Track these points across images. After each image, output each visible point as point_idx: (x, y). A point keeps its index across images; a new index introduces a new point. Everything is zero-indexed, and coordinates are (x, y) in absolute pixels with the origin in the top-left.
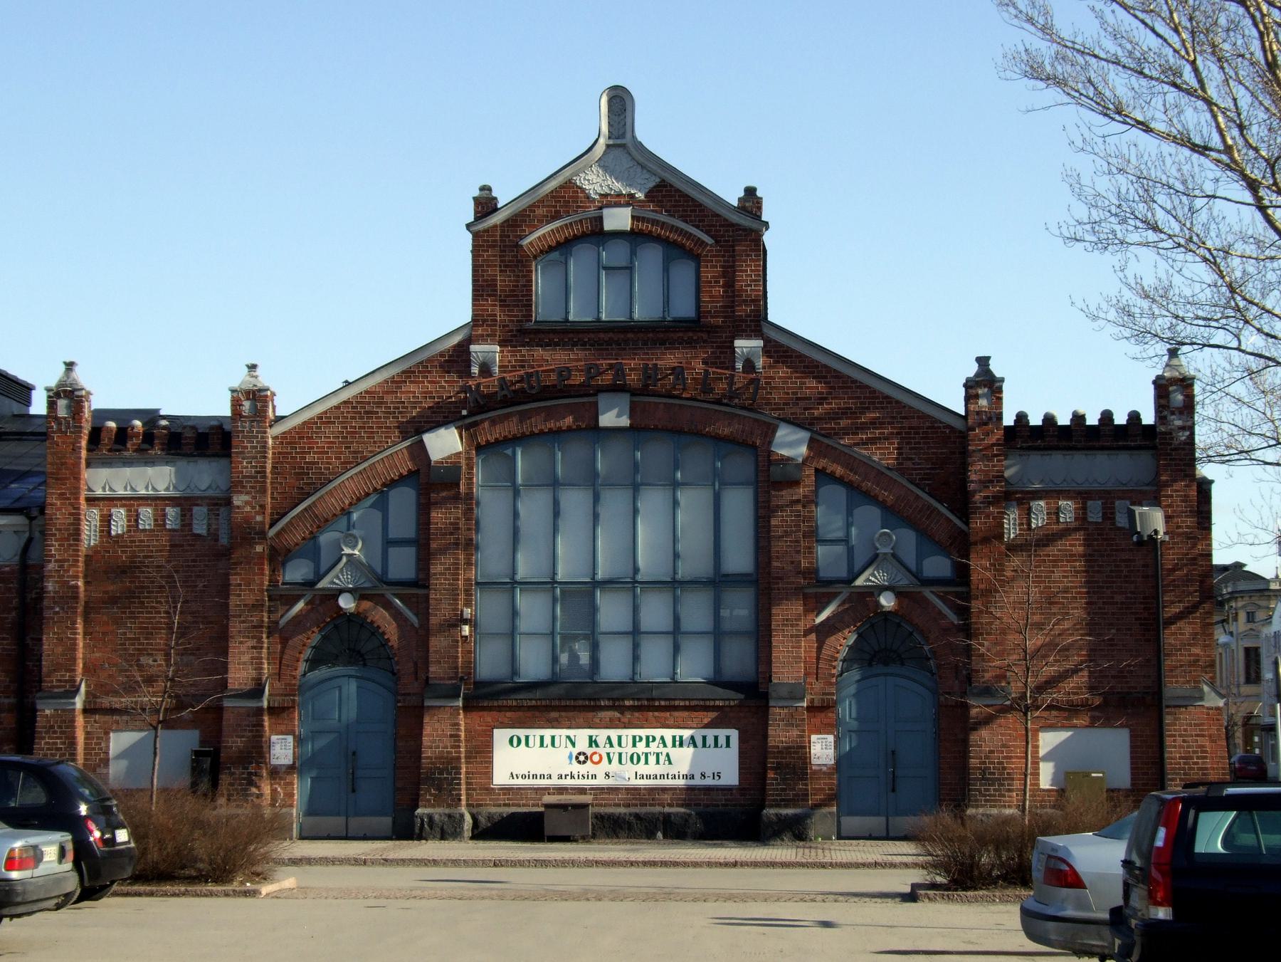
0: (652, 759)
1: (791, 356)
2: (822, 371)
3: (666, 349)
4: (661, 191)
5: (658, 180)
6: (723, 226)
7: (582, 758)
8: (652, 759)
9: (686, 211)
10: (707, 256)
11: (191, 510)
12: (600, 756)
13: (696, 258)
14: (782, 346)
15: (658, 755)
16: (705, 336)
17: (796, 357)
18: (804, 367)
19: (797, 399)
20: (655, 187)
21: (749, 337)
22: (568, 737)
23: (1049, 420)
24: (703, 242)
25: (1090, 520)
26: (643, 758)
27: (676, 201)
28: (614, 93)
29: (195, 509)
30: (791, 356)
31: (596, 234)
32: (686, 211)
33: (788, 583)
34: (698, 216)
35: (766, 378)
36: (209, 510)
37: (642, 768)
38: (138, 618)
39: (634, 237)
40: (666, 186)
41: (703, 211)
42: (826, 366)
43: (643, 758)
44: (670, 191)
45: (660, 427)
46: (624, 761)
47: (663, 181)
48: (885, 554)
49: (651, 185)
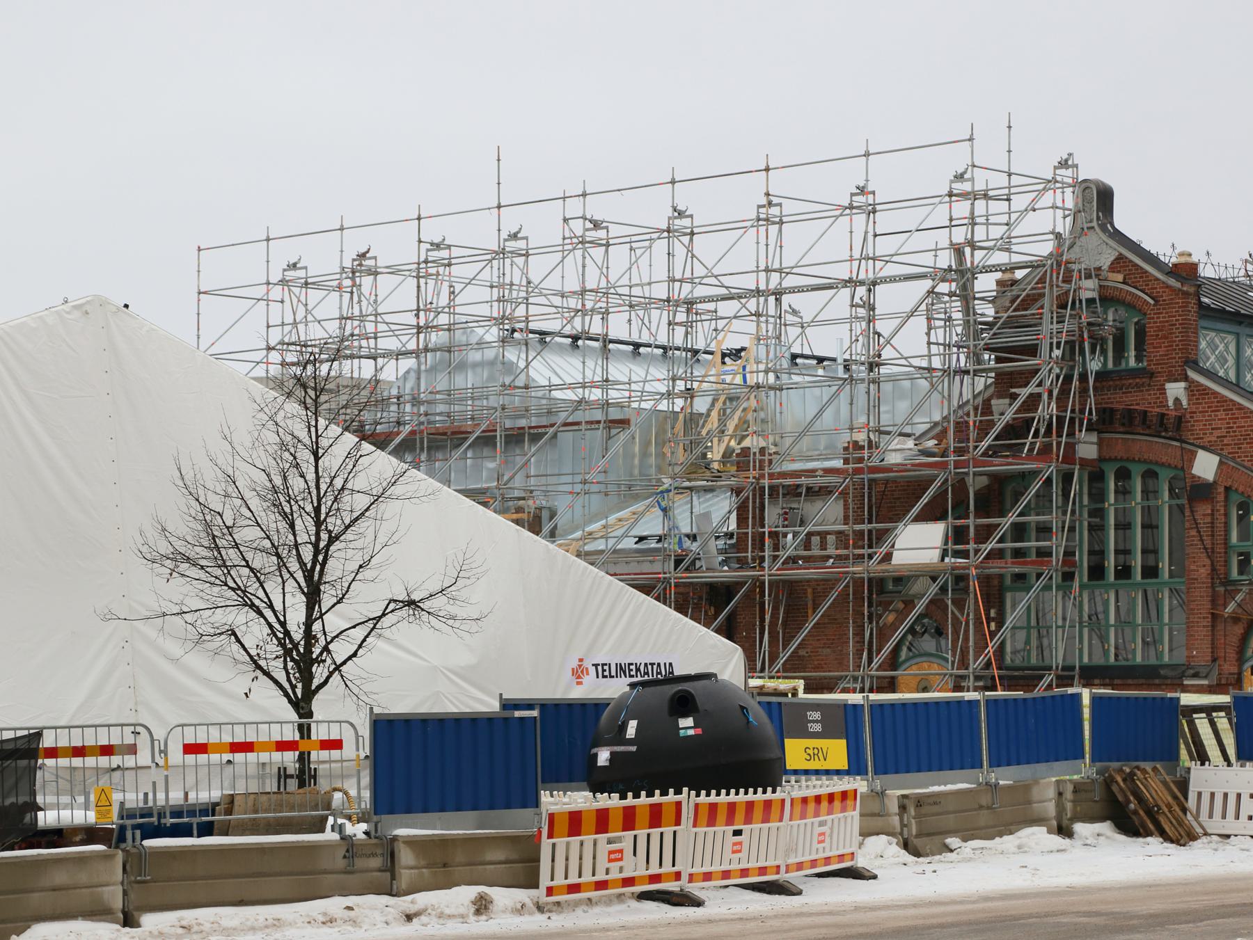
1: (1208, 394)
2: (1229, 405)
3: (1123, 393)
4: (1119, 263)
5: (1117, 254)
6: (1162, 288)
9: (1136, 278)
10: (1150, 314)
11: (826, 538)
14: (1202, 385)
17: (1212, 394)
18: (1218, 402)
19: (1212, 429)
20: (1115, 260)
21: (1176, 381)
24: (1148, 302)
27: (1129, 270)
28: (1084, 185)
29: (828, 537)
30: (1208, 394)
32: (1136, 278)
33: (1200, 583)
34: (1145, 281)
35: (1191, 413)
36: (837, 538)
38: (797, 621)
40: (1122, 258)
41: (1147, 277)
42: (1232, 401)
44: (1125, 262)
45: (1119, 457)
47: (1121, 254)
49: (1112, 258)
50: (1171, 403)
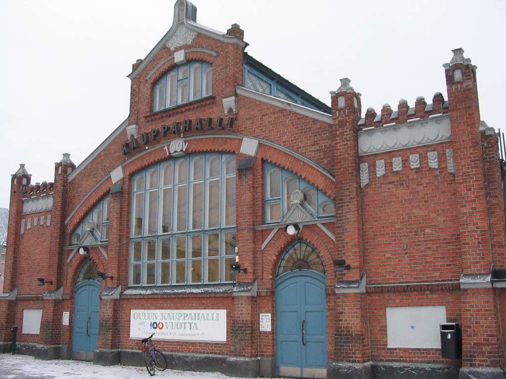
0: (188, 326)
5: (196, 34)
7: (155, 325)
8: (188, 326)
12: (162, 324)
13: (210, 64)
15: (191, 324)
16: (212, 101)
22: (154, 314)
23: (386, 110)
25: (412, 167)
26: (183, 325)
31: (175, 67)
37: (182, 331)
39: (189, 61)
43: (183, 325)
46: (174, 328)
47: (199, 33)
48: (296, 204)
50: (226, 112)
